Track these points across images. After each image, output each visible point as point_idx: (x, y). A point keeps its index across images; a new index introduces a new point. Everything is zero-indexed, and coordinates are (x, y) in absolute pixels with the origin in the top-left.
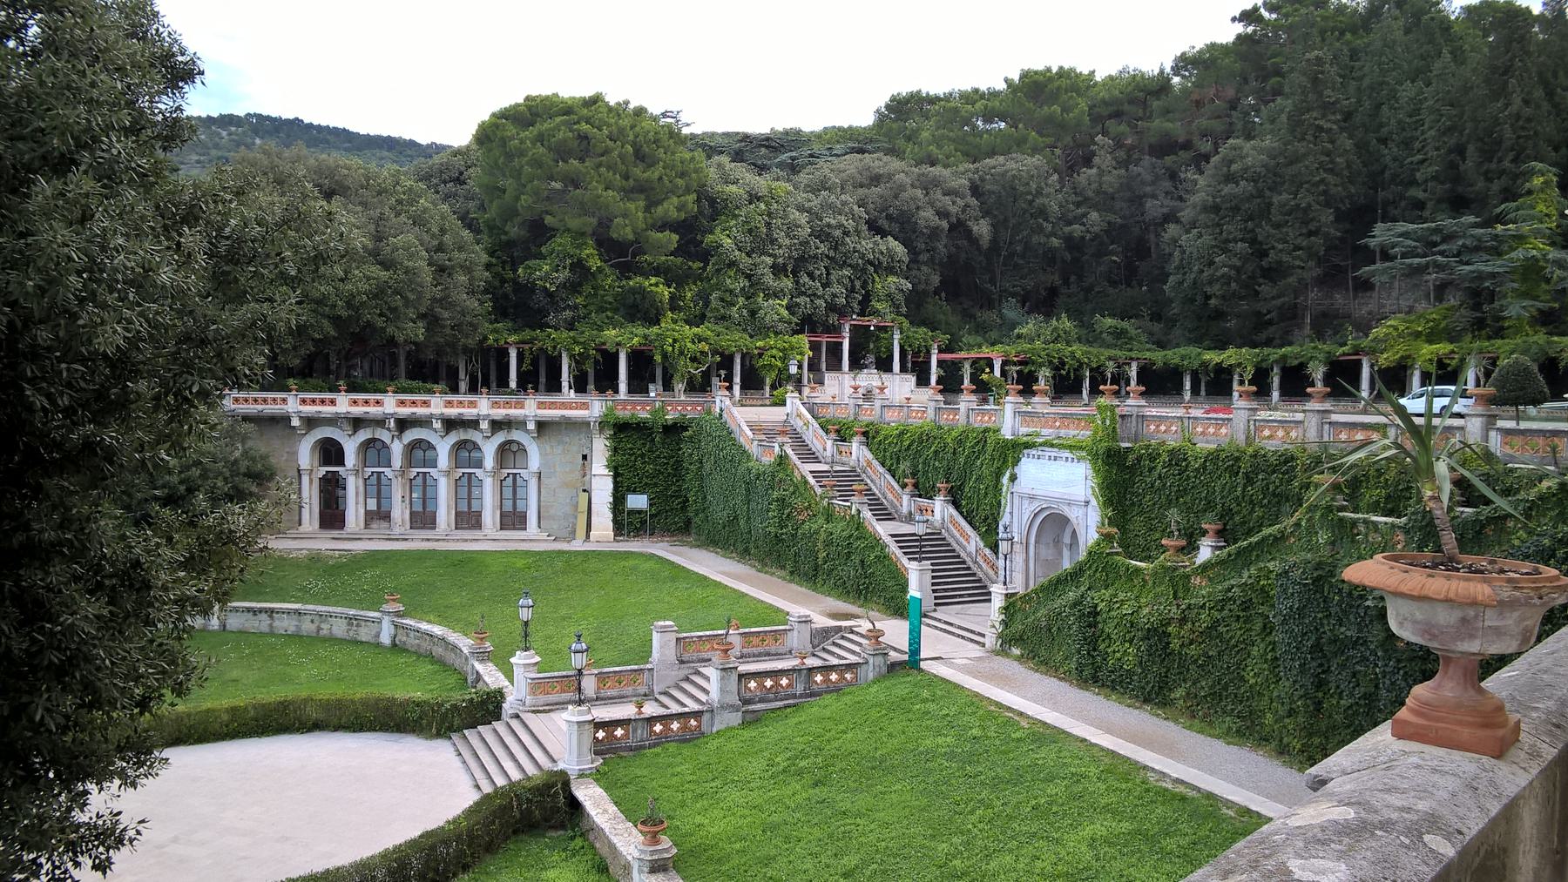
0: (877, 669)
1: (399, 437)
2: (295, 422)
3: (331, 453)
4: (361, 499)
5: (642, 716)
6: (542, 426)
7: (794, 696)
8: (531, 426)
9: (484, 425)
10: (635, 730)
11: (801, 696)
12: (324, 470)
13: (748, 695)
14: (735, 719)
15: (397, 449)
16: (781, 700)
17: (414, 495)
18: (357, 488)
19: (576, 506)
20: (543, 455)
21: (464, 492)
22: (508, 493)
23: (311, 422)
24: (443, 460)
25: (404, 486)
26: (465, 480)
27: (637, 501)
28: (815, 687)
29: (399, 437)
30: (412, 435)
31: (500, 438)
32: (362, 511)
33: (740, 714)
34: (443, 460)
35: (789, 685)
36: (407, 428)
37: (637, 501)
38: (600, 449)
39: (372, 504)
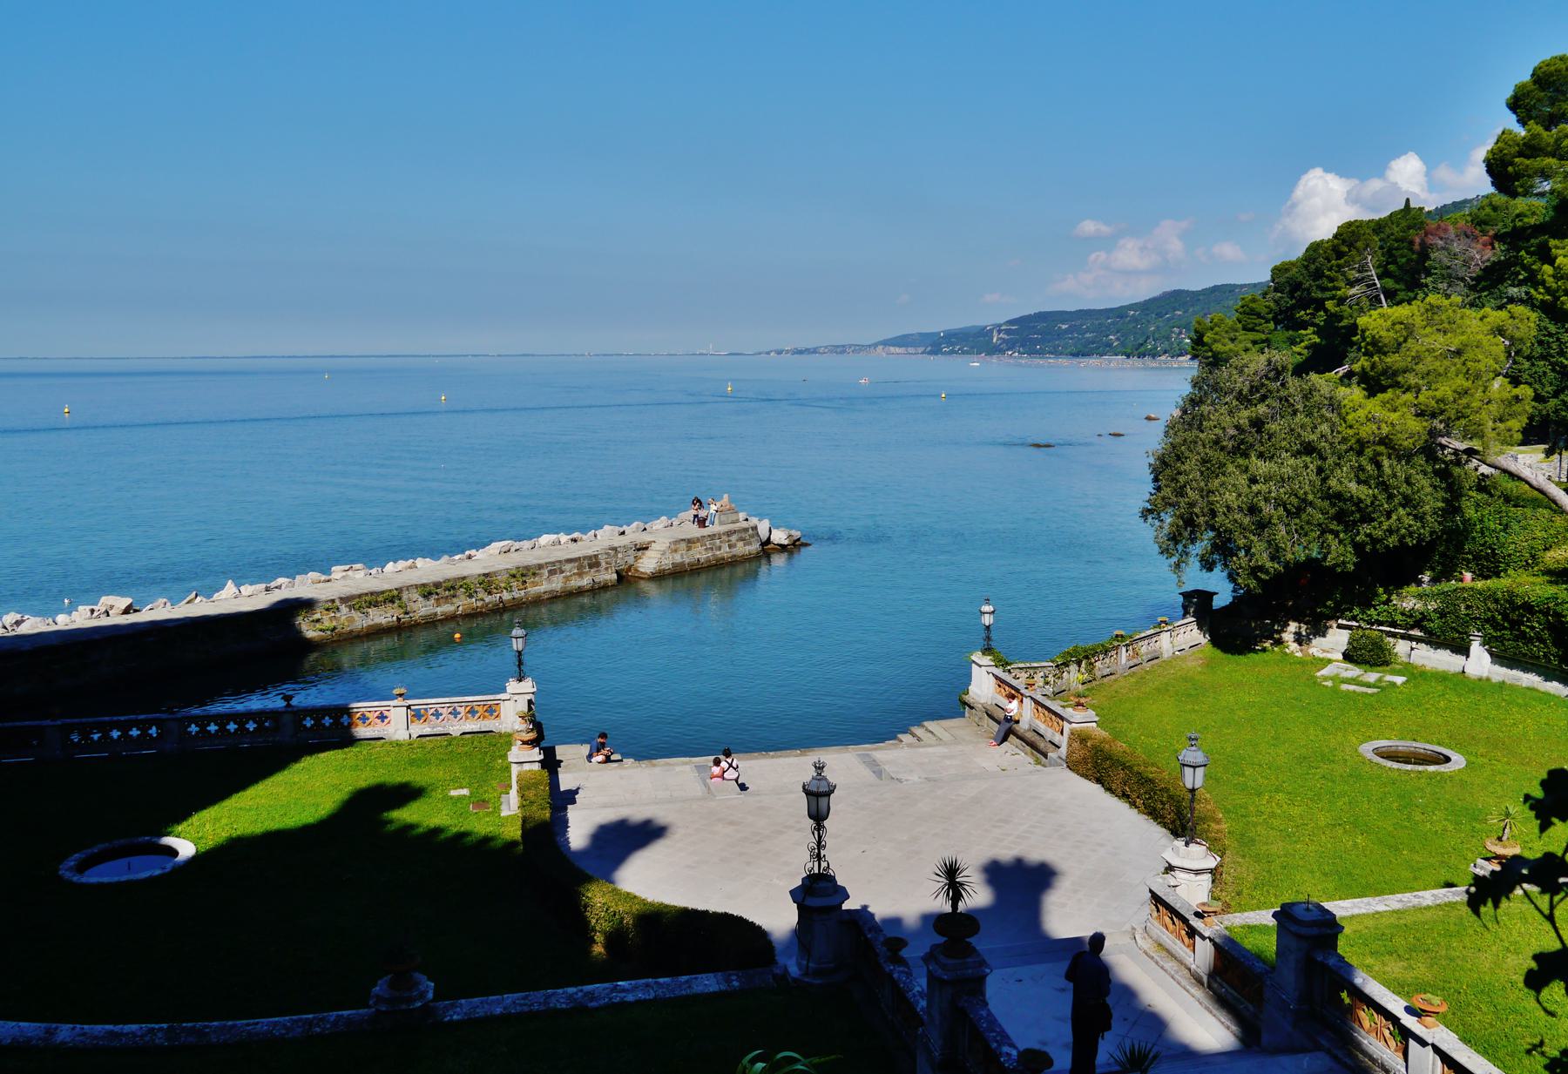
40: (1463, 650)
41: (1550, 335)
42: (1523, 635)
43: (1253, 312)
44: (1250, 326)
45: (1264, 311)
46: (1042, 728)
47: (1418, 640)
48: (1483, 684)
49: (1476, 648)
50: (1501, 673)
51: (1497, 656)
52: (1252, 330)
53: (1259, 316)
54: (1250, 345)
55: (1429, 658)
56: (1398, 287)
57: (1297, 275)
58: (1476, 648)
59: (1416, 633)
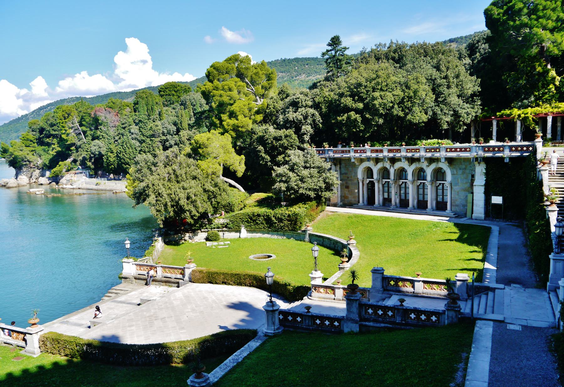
0: (450, 319)
1: (393, 167)
2: (353, 160)
3: (369, 172)
4: (381, 193)
5: (308, 314)
6: (450, 161)
7: (394, 323)
8: (443, 160)
9: (422, 160)
10: (305, 320)
11: (398, 324)
12: (368, 180)
13: (367, 316)
14: (355, 328)
15: (392, 171)
16: (385, 323)
17: (402, 192)
18: (379, 188)
19: (466, 201)
20: (453, 174)
21: (421, 191)
22: (440, 192)
23: (362, 161)
24: (410, 177)
25: (397, 187)
26: (421, 186)
27: (497, 200)
28: (409, 321)
29: (393, 167)
30: (398, 165)
31: (433, 166)
32: (381, 198)
33: (357, 325)
34: (410, 177)
35: (393, 316)
36: (396, 162)
37: (497, 200)
38: (480, 170)
39: (386, 195)
40: (239, 231)
41: (150, 145)
42: (257, 223)
43: (28, 140)
44: (28, 145)
45: (32, 139)
46: (169, 275)
47: (225, 231)
48: (246, 239)
49: (243, 230)
50: (250, 235)
51: (249, 231)
52: (29, 146)
53: (31, 141)
54: (29, 152)
55: (229, 236)
56: (87, 129)
57: (43, 125)
58: (243, 230)
59: (225, 229)
